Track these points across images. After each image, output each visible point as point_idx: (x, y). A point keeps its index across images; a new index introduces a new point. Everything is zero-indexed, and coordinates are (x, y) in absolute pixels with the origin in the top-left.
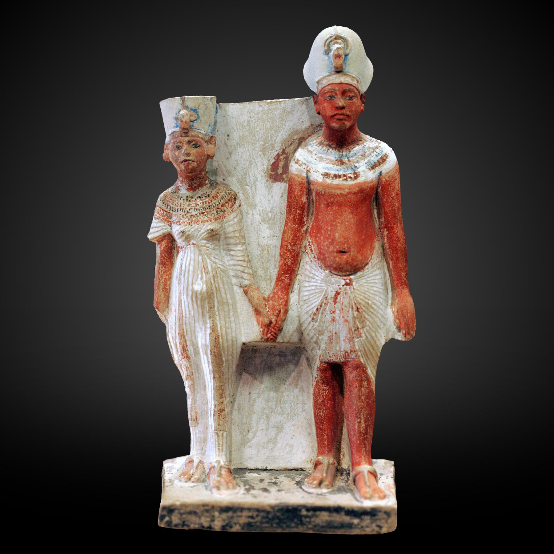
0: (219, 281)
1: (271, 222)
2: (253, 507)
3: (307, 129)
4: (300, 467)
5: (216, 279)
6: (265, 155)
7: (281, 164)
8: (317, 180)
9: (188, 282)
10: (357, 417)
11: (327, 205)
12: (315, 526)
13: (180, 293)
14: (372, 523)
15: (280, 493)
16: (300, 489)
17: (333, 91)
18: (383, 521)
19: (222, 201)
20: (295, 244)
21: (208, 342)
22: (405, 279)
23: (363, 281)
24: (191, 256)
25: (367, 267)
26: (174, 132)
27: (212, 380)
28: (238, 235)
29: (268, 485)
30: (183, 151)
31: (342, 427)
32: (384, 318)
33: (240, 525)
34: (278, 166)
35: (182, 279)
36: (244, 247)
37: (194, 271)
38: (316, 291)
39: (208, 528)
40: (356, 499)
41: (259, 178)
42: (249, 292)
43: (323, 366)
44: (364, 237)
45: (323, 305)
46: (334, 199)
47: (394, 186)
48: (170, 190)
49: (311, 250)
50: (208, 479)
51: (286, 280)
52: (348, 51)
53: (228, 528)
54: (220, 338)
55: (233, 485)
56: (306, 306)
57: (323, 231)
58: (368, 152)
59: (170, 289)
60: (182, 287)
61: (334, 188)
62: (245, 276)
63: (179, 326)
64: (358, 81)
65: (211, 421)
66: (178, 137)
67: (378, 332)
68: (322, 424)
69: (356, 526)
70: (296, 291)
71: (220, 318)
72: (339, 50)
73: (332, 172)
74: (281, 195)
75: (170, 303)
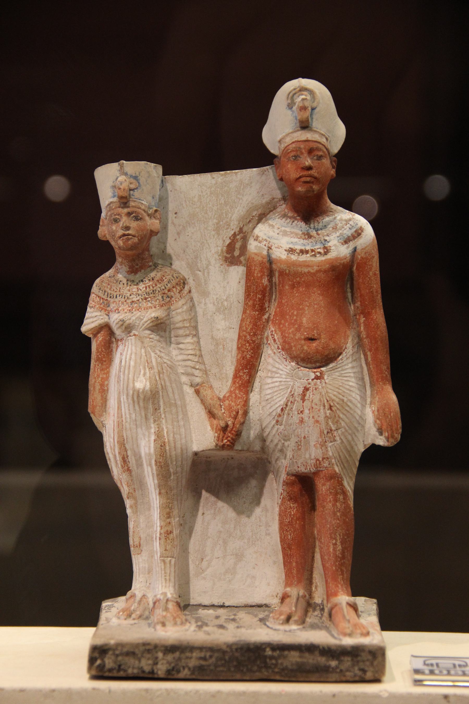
0: (166, 379)
1: (226, 312)
2: (205, 646)
3: (268, 203)
4: (264, 602)
5: (161, 375)
6: (218, 234)
7: (238, 245)
8: (279, 257)
9: (128, 379)
10: (331, 537)
11: (293, 287)
12: (283, 670)
13: (120, 392)
14: (353, 666)
15: (239, 630)
16: (263, 626)
17: (298, 150)
18: (368, 663)
19: (169, 285)
20: (255, 334)
21: (152, 450)
22: (386, 373)
23: (337, 374)
24: (132, 350)
25: (340, 357)
26: (111, 203)
27: (158, 497)
28: (188, 325)
29: (225, 622)
30: (121, 224)
31: (313, 553)
32: (362, 419)
33: (189, 669)
34: (234, 247)
35: (122, 376)
36: (195, 339)
37: (135, 367)
38: (281, 387)
39: (149, 673)
40: (333, 636)
41: (213, 261)
42: (202, 391)
43: (290, 479)
44: (336, 322)
45: (289, 404)
46: (301, 278)
47: (372, 265)
48: (107, 274)
49: (275, 340)
50: (153, 615)
51: (245, 376)
52: (314, 105)
53: (174, 672)
54: (167, 445)
55: (182, 620)
56: (269, 406)
57: (288, 317)
58: (340, 225)
59: (108, 390)
60: (122, 386)
61: (300, 266)
62: (197, 373)
63: (118, 433)
64: (327, 139)
65: (157, 546)
66: (116, 208)
67: (356, 436)
68: (290, 548)
69: (334, 670)
70: (257, 390)
71: (166, 422)
72: (305, 101)
73: (298, 247)
74: (238, 280)
75: (108, 406)
